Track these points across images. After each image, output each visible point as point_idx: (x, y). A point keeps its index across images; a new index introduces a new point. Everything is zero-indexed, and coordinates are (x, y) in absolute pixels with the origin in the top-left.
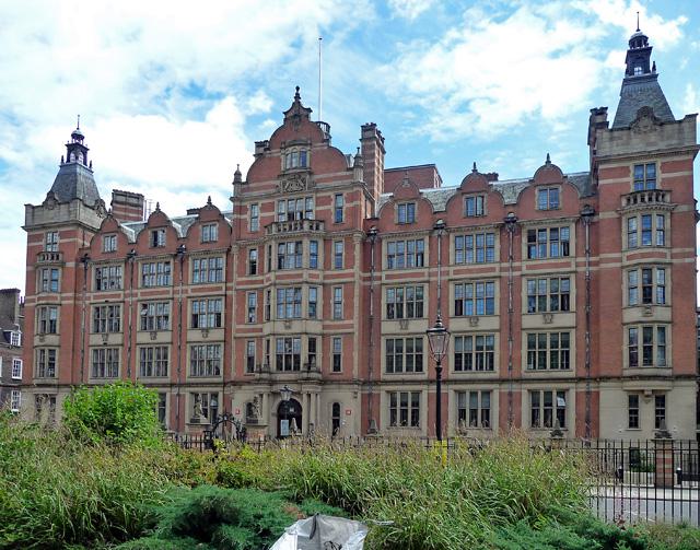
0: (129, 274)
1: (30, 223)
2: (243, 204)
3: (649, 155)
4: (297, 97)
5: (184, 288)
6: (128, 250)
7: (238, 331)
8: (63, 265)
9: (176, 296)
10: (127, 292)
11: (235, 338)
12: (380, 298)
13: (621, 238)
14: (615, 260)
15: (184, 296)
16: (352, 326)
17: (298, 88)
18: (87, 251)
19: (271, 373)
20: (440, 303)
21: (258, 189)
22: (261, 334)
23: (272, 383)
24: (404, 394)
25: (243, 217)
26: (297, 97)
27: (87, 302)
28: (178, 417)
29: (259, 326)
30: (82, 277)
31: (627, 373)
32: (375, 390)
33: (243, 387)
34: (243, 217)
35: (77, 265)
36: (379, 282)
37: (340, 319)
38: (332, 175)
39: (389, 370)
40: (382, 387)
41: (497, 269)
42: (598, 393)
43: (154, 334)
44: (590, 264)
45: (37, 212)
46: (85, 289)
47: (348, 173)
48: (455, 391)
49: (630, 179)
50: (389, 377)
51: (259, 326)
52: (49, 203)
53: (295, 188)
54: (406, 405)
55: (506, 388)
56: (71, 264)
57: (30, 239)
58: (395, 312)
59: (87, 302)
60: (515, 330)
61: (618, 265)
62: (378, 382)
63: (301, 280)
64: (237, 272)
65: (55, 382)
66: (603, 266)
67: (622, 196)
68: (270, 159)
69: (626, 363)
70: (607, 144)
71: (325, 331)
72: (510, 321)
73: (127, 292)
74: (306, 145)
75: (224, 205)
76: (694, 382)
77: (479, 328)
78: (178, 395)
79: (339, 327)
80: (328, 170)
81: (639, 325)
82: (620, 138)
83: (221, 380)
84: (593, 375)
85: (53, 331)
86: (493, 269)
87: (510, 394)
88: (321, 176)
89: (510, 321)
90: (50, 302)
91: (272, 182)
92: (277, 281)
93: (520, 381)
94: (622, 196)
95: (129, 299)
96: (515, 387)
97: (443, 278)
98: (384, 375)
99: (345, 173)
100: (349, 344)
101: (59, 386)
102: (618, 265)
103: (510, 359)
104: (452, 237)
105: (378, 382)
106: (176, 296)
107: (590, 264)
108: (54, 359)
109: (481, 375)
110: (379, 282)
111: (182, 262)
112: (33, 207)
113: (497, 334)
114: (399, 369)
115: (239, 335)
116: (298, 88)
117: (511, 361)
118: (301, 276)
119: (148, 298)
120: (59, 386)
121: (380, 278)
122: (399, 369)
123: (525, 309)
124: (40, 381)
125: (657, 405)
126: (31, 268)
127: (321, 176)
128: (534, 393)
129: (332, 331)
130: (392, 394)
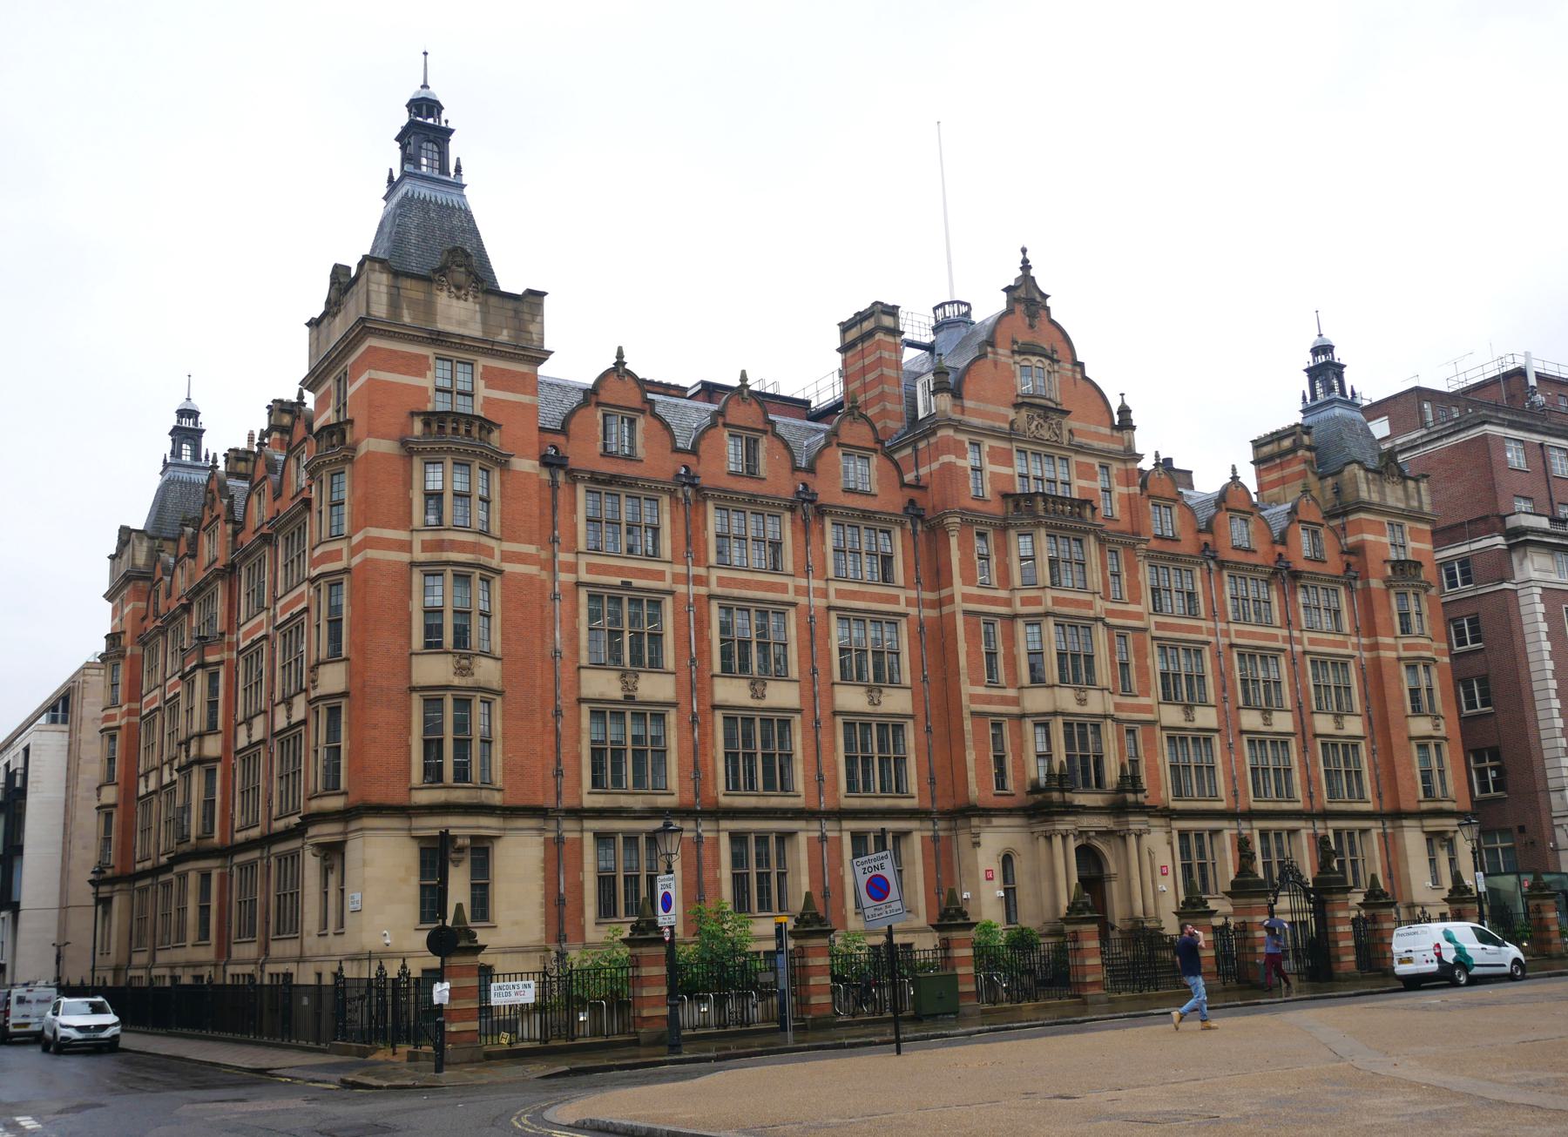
11: (973, 713)
17: (1024, 251)
22: (1014, 710)
26: (1025, 262)
29: (1011, 692)
33: (995, 821)
43: (873, 691)
49: (1387, 540)
51: (1011, 692)
60: (1309, 736)
63: (1091, 613)
69: (1421, 795)
77: (1276, 728)
92: (1058, 609)
116: (1024, 251)
119: (736, 592)
125: (474, 874)
128: (737, 838)
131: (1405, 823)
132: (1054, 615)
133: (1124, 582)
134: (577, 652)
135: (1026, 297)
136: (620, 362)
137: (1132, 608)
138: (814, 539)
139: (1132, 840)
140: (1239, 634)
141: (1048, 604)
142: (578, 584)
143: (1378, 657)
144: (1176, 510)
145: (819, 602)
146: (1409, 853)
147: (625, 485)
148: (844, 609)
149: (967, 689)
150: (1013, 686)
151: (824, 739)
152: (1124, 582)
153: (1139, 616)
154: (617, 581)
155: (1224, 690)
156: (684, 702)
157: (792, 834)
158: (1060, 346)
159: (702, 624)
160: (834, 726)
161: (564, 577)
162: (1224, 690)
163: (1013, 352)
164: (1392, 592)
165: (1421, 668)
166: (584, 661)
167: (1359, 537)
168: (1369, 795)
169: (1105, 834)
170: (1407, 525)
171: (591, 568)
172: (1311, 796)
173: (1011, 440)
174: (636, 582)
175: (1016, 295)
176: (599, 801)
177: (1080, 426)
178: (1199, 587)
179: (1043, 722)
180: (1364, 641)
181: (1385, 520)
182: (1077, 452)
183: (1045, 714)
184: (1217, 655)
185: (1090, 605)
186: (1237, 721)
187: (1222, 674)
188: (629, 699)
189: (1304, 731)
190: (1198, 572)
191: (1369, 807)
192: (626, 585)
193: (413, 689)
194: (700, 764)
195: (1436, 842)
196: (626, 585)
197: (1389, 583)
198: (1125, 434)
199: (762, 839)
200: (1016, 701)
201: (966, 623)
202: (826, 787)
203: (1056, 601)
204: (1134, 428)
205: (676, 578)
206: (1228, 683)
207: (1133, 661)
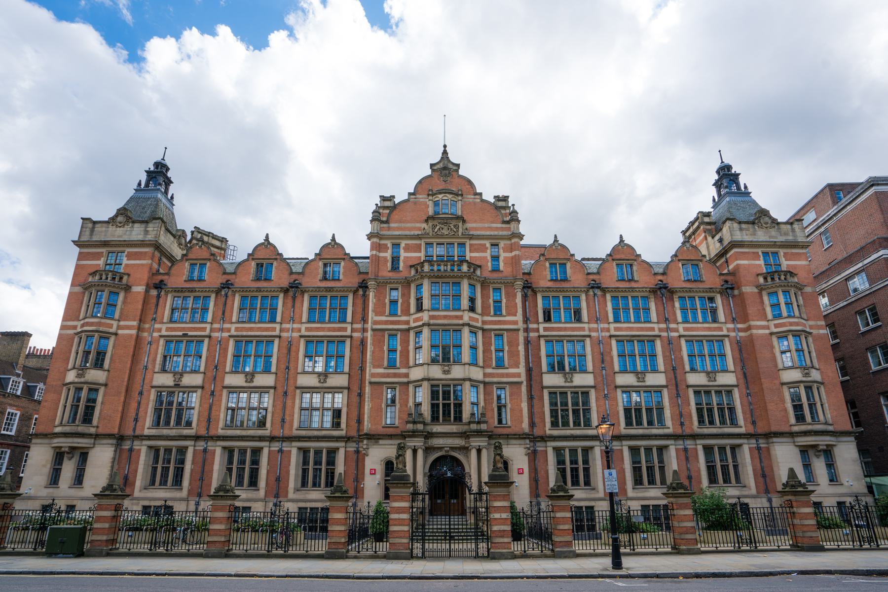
0: (221, 306)
1: (85, 238)
2: (383, 242)
3: (774, 245)
4: (445, 152)
5: (295, 326)
6: (223, 279)
7: (373, 375)
8: (128, 288)
9: (284, 335)
10: (216, 326)
11: (370, 383)
12: (539, 350)
13: (764, 309)
14: (763, 327)
15: (296, 335)
16: (519, 375)
18: (165, 278)
19: (425, 424)
20: (603, 359)
21: (398, 229)
22: (405, 380)
23: (429, 435)
24: (573, 451)
25: (382, 255)
26: (445, 152)
27: (156, 334)
28: (278, 479)
29: (403, 371)
30: (152, 306)
31: (796, 429)
32: (540, 447)
33: (381, 442)
34: (382, 255)
35: (147, 291)
36: (536, 334)
37: (503, 367)
38: (486, 225)
39: (554, 424)
40: (549, 444)
41: (656, 329)
42: (768, 449)
44: (740, 330)
45: (98, 228)
46: (154, 319)
47: (504, 226)
50: (556, 433)
51: (403, 371)
52: (120, 219)
53: (445, 232)
54: (576, 463)
56: (139, 289)
57: (81, 257)
58: (558, 367)
59: (156, 334)
60: (682, 387)
61: (767, 332)
62: (544, 439)
63: (461, 322)
64: (373, 311)
65: (93, 430)
66: (754, 331)
67: (758, 275)
68: (415, 203)
69: (793, 420)
70: (738, 233)
71: (487, 380)
72: (676, 377)
73: (216, 326)
74: (457, 195)
75: (358, 245)
76: (853, 439)
77: (647, 384)
78: (281, 451)
79: (502, 375)
80: (482, 221)
81: (802, 385)
82: (747, 230)
83: (343, 433)
84: (760, 431)
85: (99, 364)
86: (653, 329)
88: (474, 225)
89: (676, 377)
90: (101, 329)
91: (418, 225)
92: (432, 322)
93: (694, 437)
94: (758, 275)
95: (215, 335)
96: (689, 443)
97: (604, 334)
98: (549, 431)
99: (500, 225)
100: (515, 395)
101: (97, 436)
102: (767, 332)
103: (681, 415)
104: (608, 297)
105: (544, 439)
106: (284, 335)
107: (740, 330)
108: (94, 401)
110: (536, 334)
111: (294, 298)
112: (95, 223)
114: (566, 424)
115: (373, 380)
117: (681, 417)
118: (461, 317)
119: (245, 333)
120: (97, 436)
121: (537, 330)
122: (566, 424)
123: (687, 368)
124: (67, 429)
126: (78, 289)
127: (474, 225)
129: (495, 380)
130: (558, 451)
131: (775, 440)
134: (154, 367)
135: (445, 169)
138: (298, 304)
143: (751, 335)
145: (296, 335)
146: (779, 460)
147: (192, 291)
148: (309, 336)
149: (369, 370)
150: (405, 367)
151: (289, 402)
154: (180, 333)
155: (603, 362)
156: (206, 386)
158: (466, 188)
160: (295, 395)
162: (603, 362)
163: (428, 195)
164: (764, 293)
165: (803, 337)
167: (735, 263)
168: (741, 422)
170: (782, 252)
171: (168, 329)
172: (682, 424)
173: (420, 238)
174: (190, 333)
176: (154, 432)
178: (584, 305)
179: (418, 383)
180: (740, 326)
181: (760, 251)
183: (418, 381)
186: (614, 381)
187: (602, 354)
189: (676, 384)
190: (583, 297)
191: (742, 430)
192: (185, 335)
194: (213, 417)
195: (811, 453)
196: (185, 335)
197: (761, 288)
198: (513, 225)
200: (407, 375)
201: (374, 336)
202: (287, 426)
204: (519, 221)
206: (607, 358)
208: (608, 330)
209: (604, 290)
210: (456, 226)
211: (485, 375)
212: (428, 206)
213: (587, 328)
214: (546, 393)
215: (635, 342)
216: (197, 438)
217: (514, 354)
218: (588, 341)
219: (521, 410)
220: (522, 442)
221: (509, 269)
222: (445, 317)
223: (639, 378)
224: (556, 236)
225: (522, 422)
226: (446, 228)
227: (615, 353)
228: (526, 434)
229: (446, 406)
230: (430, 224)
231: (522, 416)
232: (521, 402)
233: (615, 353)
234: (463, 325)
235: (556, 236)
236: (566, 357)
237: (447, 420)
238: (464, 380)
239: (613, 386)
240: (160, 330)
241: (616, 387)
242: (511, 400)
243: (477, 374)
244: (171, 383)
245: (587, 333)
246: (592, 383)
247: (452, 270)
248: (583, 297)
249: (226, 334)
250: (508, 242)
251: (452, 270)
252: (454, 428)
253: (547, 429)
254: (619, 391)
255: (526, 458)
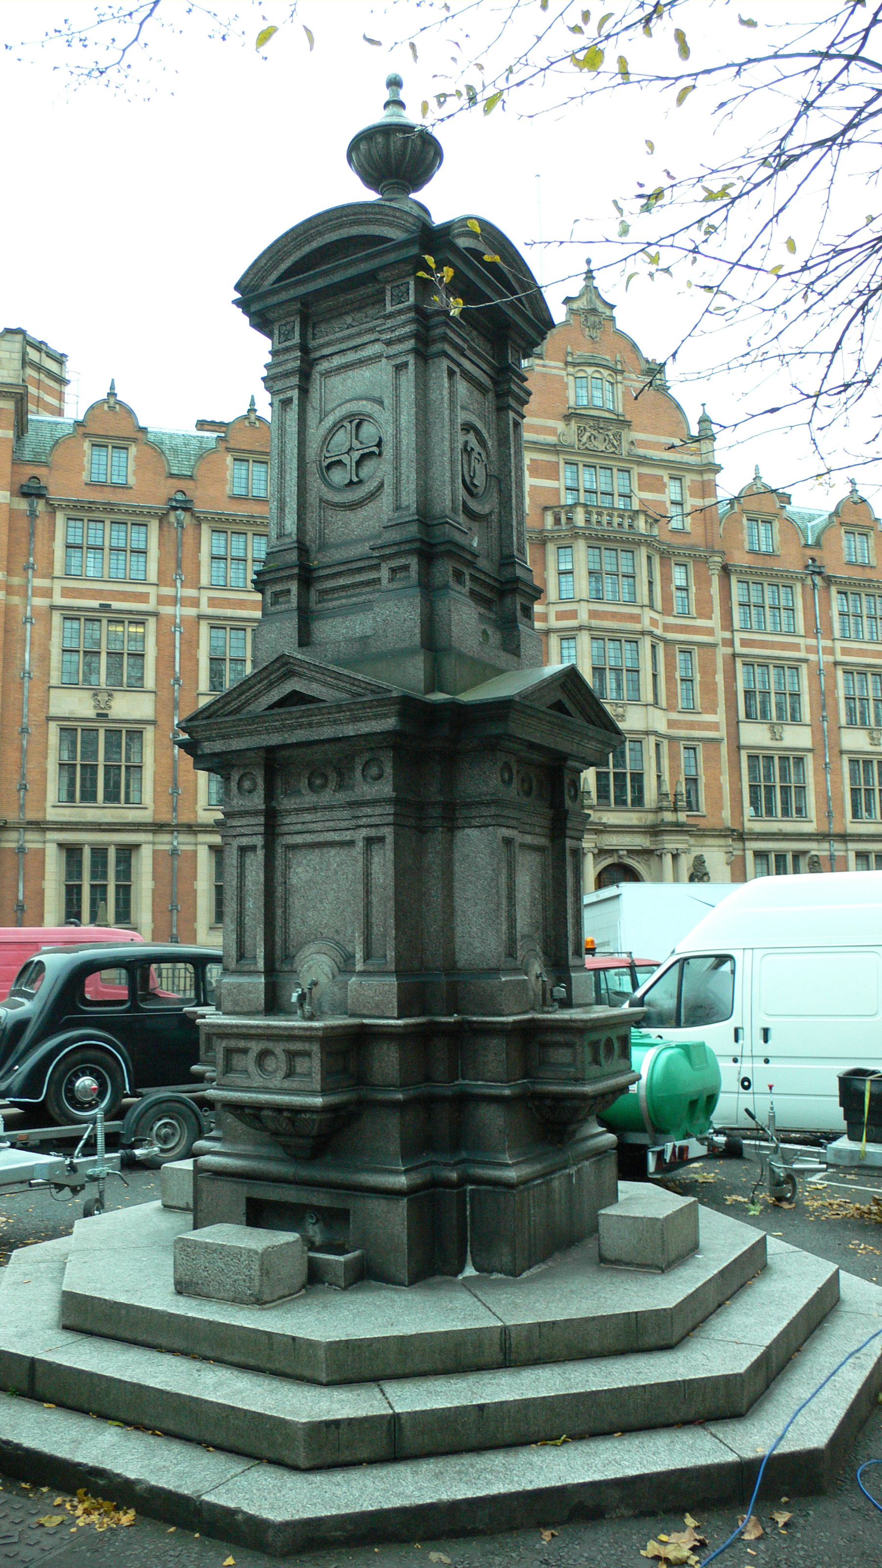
16: (715, 726)
20: (824, 701)
48: (60, 845)
55: (165, 841)
74: (616, 371)
79: (692, 725)
80: (655, 430)
87: (174, 852)
91: (551, 423)
92: (595, 623)
100: (713, 760)
109: (789, 827)
113: (810, 756)
119: (229, 612)
132: (590, 629)
133: (692, 596)
136: (112, 394)
137: (700, 622)
139: (668, 859)
140: (845, 651)
141: (583, 617)
142: (53, 608)
144: (776, 524)
152: (692, 596)
153: (710, 632)
154: (95, 604)
155: (824, 707)
156: (162, 720)
157: (137, 846)
159: (191, 644)
161: (38, 601)
162: (824, 707)
166: (54, 681)
169: (646, 853)
171: (66, 592)
173: (558, 453)
174: (116, 605)
175: (575, 306)
177: (646, 438)
182: (640, 464)
184: (817, 672)
185: (636, 618)
187: (822, 693)
188: (102, 716)
190: (798, 588)
192: (105, 608)
193: (49, 719)
196: (105, 608)
199: (99, 853)
203: (593, 614)
205: (161, 600)
206: (829, 701)
207: (698, 677)
208: (831, 651)
209: (829, 580)
210: (618, 436)
211: (671, 724)
212: (566, 386)
213: (803, 647)
214: (744, 754)
215: (869, 675)
216: (157, 827)
217: (709, 688)
218: (804, 669)
219: (720, 788)
220: (721, 842)
221: (700, 530)
222: (614, 616)
223: (872, 739)
224: (757, 469)
225: (722, 808)
226: (601, 437)
227: (841, 693)
228: (728, 829)
229: (620, 778)
230: (574, 425)
231: (721, 798)
232: (720, 774)
233: (841, 693)
234: (643, 633)
235: (757, 469)
236: (773, 695)
237: (621, 801)
238: (647, 733)
239: (836, 751)
240: (48, 593)
241: (842, 752)
242: (706, 769)
243: (659, 721)
244: (91, 713)
245: (802, 655)
246: (808, 744)
247: (610, 523)
248: (798, 588)
249: (191, 612)
250: (697, 478)
251: (610, 523)
252: (631, 818)
253: (746, 819)
254: (845, 758)
255: (728, 868)
